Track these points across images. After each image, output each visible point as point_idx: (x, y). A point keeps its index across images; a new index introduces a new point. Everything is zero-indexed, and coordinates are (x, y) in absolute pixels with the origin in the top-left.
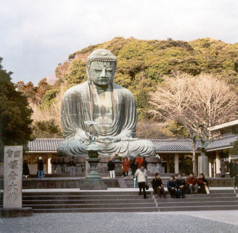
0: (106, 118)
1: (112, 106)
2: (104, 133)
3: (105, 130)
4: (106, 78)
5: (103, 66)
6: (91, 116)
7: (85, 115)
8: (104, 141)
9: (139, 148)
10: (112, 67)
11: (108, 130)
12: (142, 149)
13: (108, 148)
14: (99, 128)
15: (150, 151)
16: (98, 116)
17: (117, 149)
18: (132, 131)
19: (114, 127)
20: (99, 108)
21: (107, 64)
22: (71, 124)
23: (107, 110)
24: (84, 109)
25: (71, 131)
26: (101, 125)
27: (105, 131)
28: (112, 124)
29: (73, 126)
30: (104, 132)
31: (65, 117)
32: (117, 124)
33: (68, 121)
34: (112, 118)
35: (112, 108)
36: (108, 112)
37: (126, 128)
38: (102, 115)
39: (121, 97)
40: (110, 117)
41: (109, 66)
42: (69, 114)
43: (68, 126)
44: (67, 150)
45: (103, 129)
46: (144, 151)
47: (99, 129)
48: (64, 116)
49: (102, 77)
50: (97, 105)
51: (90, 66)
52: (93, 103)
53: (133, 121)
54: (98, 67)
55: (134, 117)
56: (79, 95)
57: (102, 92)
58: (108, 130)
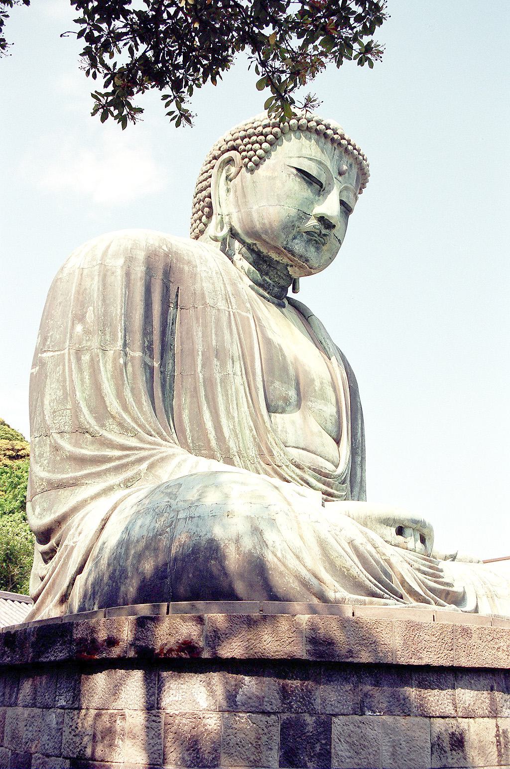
7: (218, 376)
14: (298, 466)
22: (125, 408)
23: (317, 384)
24: (214, 343)
25: (123, 448)
29: (135, 420)
31: (86, 358)
33: (108, 388)
42: (120, 343)
43: (102, 413)
44: (298, 543)
45: (319, 481)
48: (78, 353)
49: (322, 219)
51: (266, 152)
56: (186, 268)
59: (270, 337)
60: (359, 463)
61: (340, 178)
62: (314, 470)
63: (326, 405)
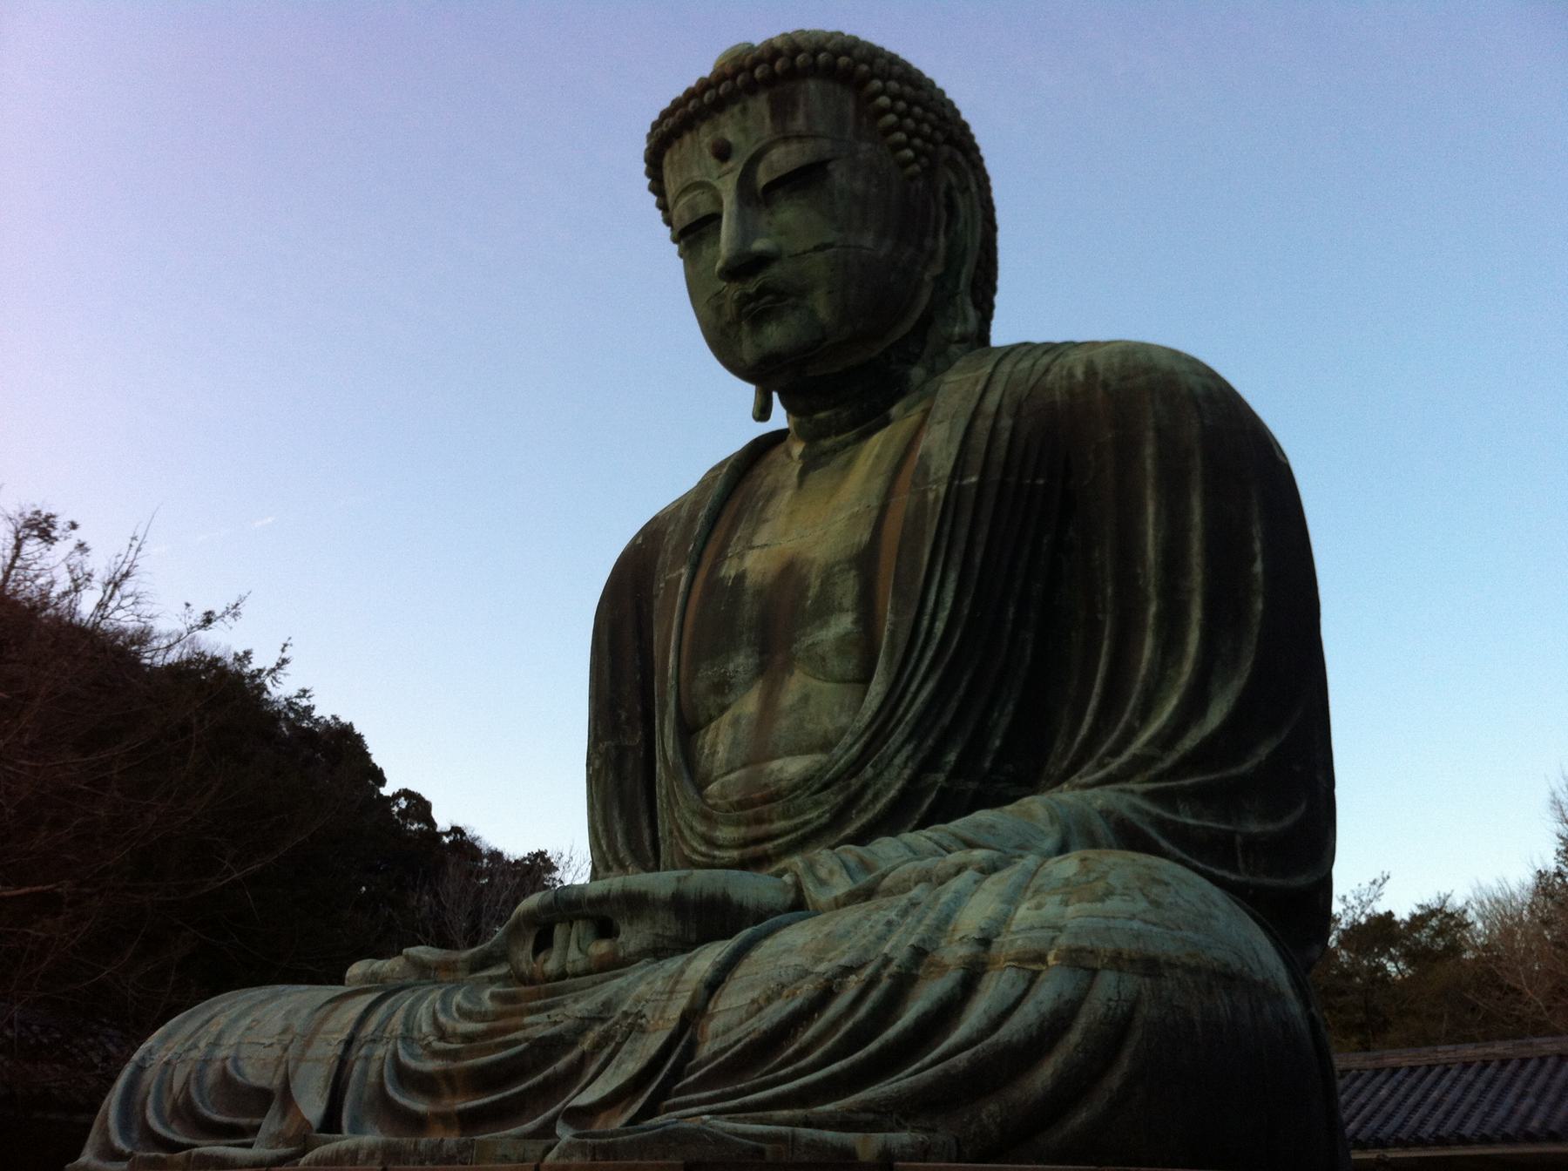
0: (796, 685)
1: (866, 537)
2: (742, 865)
3: (748, 825)
4: (775, 270)
5: (712, 162)
6: (664, 705)
8: (541, 956)
9: (826, 994)
10: (799, 137)
11: (780, 825)
12: (874, 995)
13: (516, 1042)
14: (707, 817)
15: (1004, 1033)
16: (723, 687)
17: (598, 1046)
18: (1150, 795)
19: (869, 771)
20: (748, 598)
21: (744, 130)
23: (812, 593)
26: (732, 777)
27: (744, 844)
28: (848, 739)
30: (735, 854)
32: (917, 732)
34: (850, 667)
35: (865, 561)
36: (825, 610)
37: (1086, 768)
38: (761, 670)
39: (1006, 422)
40: (835, 665)
41: (767, 129)
45: (738, 823)
46: (873, 1046)
47: (701, 828)
50: (740, 577)
52: (716, 567)
53: (1188, 667)
54: (685, 190)
55: (1196, 613)
57: (846, 445)
58: (786, 815)
59: (723, 573)
60: (1151, 620)
61: (730, 164)
62: (741, 805)
63: (825, 624)
